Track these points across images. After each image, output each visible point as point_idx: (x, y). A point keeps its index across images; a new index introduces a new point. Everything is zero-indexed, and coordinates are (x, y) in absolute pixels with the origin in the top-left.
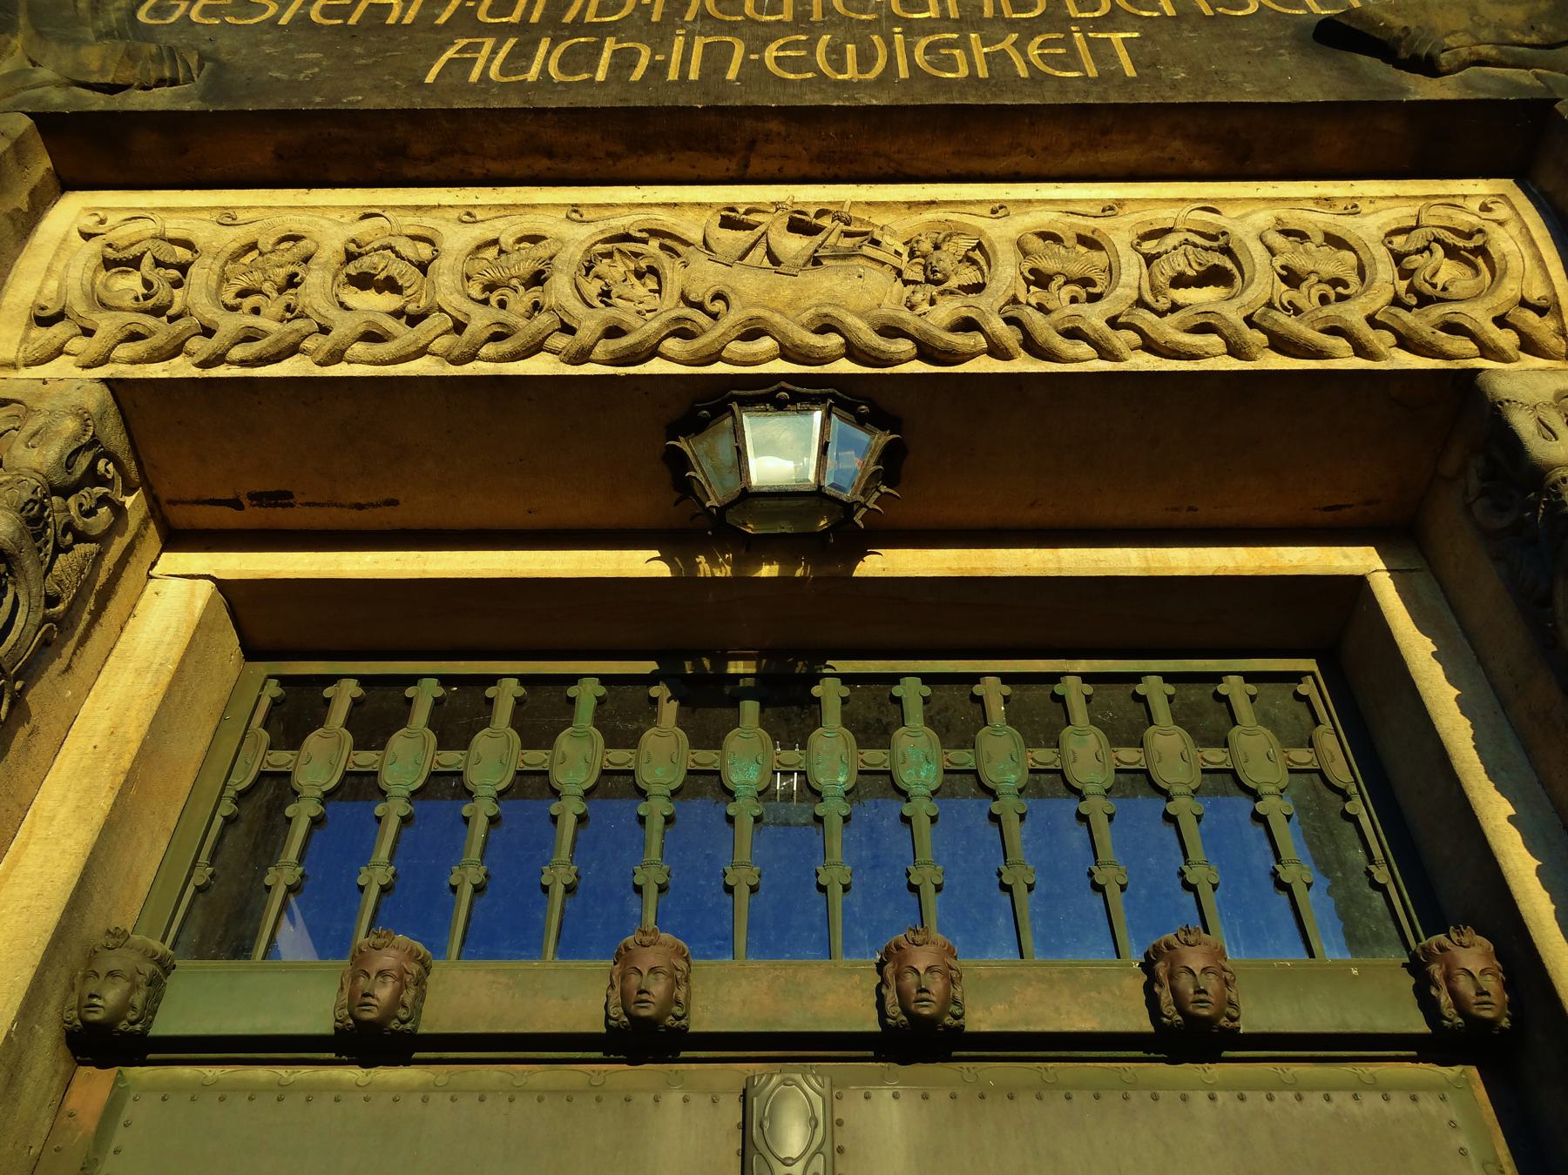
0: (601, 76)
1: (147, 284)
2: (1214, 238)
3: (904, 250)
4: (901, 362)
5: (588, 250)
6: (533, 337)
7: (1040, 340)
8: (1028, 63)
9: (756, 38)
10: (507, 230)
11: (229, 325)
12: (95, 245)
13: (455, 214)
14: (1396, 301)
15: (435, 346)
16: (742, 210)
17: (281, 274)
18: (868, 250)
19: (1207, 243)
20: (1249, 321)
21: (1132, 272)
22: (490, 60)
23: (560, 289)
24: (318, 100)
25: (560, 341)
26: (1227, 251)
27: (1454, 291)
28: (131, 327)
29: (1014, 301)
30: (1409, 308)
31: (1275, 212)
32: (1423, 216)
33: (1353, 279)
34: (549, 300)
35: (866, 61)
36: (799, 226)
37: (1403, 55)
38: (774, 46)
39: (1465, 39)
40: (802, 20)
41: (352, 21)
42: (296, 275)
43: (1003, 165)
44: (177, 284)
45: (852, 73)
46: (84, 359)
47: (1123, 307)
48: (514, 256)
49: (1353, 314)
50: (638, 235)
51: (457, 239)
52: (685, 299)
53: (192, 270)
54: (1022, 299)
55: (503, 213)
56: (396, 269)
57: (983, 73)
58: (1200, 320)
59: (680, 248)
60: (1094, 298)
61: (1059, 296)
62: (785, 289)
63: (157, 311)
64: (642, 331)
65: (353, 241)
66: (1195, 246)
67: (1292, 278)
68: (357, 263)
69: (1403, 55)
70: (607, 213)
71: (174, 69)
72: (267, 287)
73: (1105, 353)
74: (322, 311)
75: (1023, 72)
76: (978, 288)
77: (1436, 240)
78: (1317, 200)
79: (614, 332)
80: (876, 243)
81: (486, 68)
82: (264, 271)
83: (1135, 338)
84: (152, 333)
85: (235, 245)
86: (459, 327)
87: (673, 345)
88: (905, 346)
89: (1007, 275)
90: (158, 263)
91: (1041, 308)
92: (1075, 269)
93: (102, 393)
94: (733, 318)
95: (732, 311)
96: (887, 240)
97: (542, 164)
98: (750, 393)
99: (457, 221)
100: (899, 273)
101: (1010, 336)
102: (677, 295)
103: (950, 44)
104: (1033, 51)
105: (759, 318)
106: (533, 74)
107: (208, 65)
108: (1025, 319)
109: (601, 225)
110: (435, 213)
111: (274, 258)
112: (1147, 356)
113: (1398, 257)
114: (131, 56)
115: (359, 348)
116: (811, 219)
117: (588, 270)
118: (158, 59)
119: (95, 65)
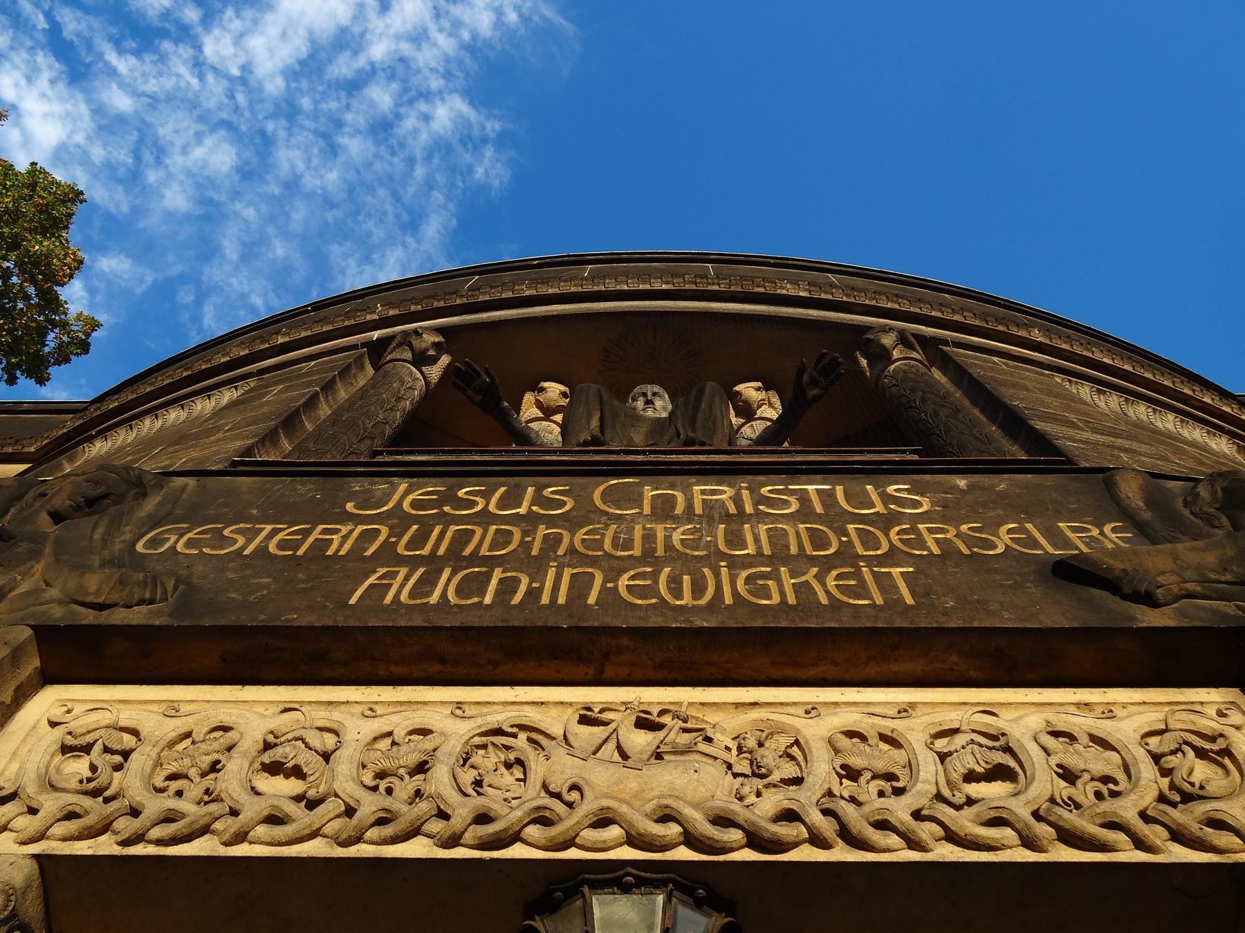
0: (488, 600)
1: (93, 768)
2: (994, 738)
3: (733, 745)
4: (732, 850)
5: (466, 743)
6: (412, 823)
7: (854, 831)
8: (827, 592)
9: (612, 569)
10: (400, 724)
11: (154, 806)
12: (59, 732)
13: (359, 708)
14: (1162, 798)
15: (326, 830)
16: (597, 710)
17: (206, 761)
18: (703, 747)
19: (991, 743)
20: (1036, 815)
21: (929, 769)
22: (402, 586)
23: (440, 780)
24: (262, 617)
25: (436, 826)
26: (1007, 749)
27: (1211, 789)
28: (70, 808)
29: (830, 793)
30: (1174, 805)
31: (1044, 716)
32: (1170, 721)
33: (1120, 776)
34: (429, 789)
35: (698, 590)
36: (643, 723)
37: (1126, 590)
38: (626, 576)
39: (1173, 578)
40: (648, 555)
41: (300, 553)
42: (219, 762)
43: (812, 672)
44: (118, 768)
45: (687, 599)
46: (23, 836)
47: (924, 802)
48: (404, 748)
49: (1127, 809)
50: (510, 730)
51: (358, 730)
52: (545, 787)
53: (133, 756)
54: (837, 792)
55: (399, 709)
56: (305, 759)
57: (791, 600)
58: (993, 814)
59: (544, 741)
60: (899, 792)
61: (869, 789)
62: (632, 781)
63: (95, 793)
64: (509, 817)
65: (272, 732)
66: (981, 745)
67: (1068, 775)
68: (271, 752)
69: (1126, 590)
70: (485, 710)
71: (154, 592)
72: (193, 772)
73: (913, 843)
74: (235, 795)
75: (824, 600)
76: (798, 781)
77: (1186, 743)
78: (1078, 705)
79: (483, 818)
80: (708, 740)
81: (399, 592)
82: (193, 757)
83: (939, 831)
84: (87, 813)
85: (174, 734)
86: (350, 812)
87: (533, 831)
88: (736, 835)
89: (821, 771)
90: (106, 750)
91: (853, 800)
92: (880, 766)
93: (31, 867)
94: (587, 807)
95: (585, 801)
96: (718, 737)
97: (436, 668)
98: (599, 877)
99: (359, 717)
100: (729, 766)
101: (827, 827)
102: (539, 785)
103: (765, 576)
104: (831, 582)
105: (608, 808)
106: (434, 598)
107: (182, 587)
108: (840, 812)
109: (479, 721)
110: (343, 708)
111: (203, 747)
112: (950, 847)
113: (1156, 758)
114: (122, 582)
115: (261, 831)
116: (654, 717)
117: (465, 760)
118: (144, 584)
119: (93, 588)
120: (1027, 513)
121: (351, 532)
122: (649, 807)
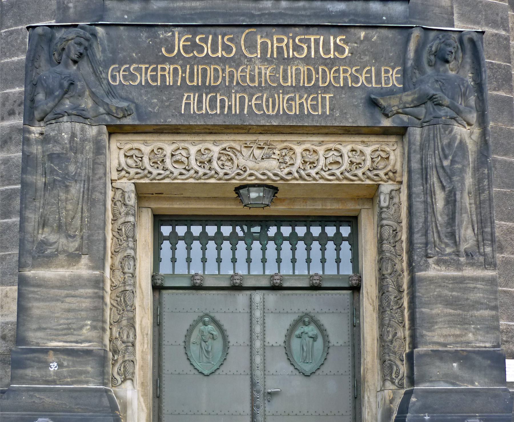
10: (202, 147)
24: (162, 121)
29: (299, 168)
45: (271, 113)
75: (306, 113)
88: (278, 178)
99: (193, 147)
120: (376, 60)
121: (170, 69)
122: (261, 172)
